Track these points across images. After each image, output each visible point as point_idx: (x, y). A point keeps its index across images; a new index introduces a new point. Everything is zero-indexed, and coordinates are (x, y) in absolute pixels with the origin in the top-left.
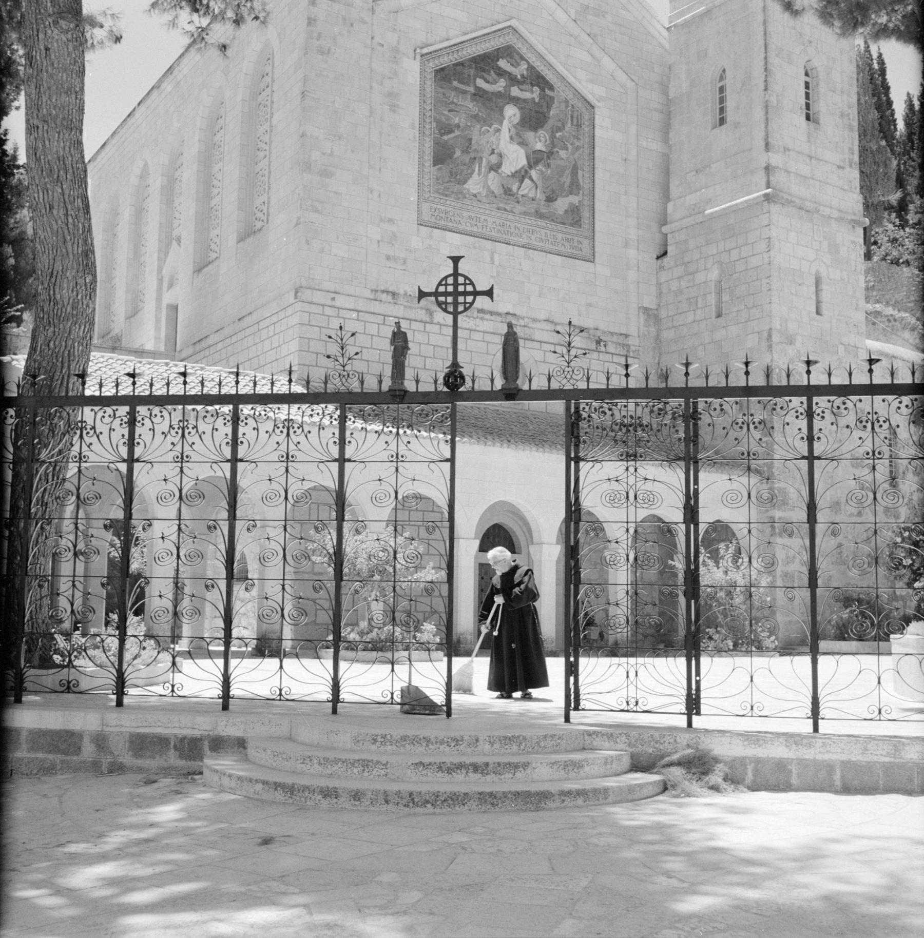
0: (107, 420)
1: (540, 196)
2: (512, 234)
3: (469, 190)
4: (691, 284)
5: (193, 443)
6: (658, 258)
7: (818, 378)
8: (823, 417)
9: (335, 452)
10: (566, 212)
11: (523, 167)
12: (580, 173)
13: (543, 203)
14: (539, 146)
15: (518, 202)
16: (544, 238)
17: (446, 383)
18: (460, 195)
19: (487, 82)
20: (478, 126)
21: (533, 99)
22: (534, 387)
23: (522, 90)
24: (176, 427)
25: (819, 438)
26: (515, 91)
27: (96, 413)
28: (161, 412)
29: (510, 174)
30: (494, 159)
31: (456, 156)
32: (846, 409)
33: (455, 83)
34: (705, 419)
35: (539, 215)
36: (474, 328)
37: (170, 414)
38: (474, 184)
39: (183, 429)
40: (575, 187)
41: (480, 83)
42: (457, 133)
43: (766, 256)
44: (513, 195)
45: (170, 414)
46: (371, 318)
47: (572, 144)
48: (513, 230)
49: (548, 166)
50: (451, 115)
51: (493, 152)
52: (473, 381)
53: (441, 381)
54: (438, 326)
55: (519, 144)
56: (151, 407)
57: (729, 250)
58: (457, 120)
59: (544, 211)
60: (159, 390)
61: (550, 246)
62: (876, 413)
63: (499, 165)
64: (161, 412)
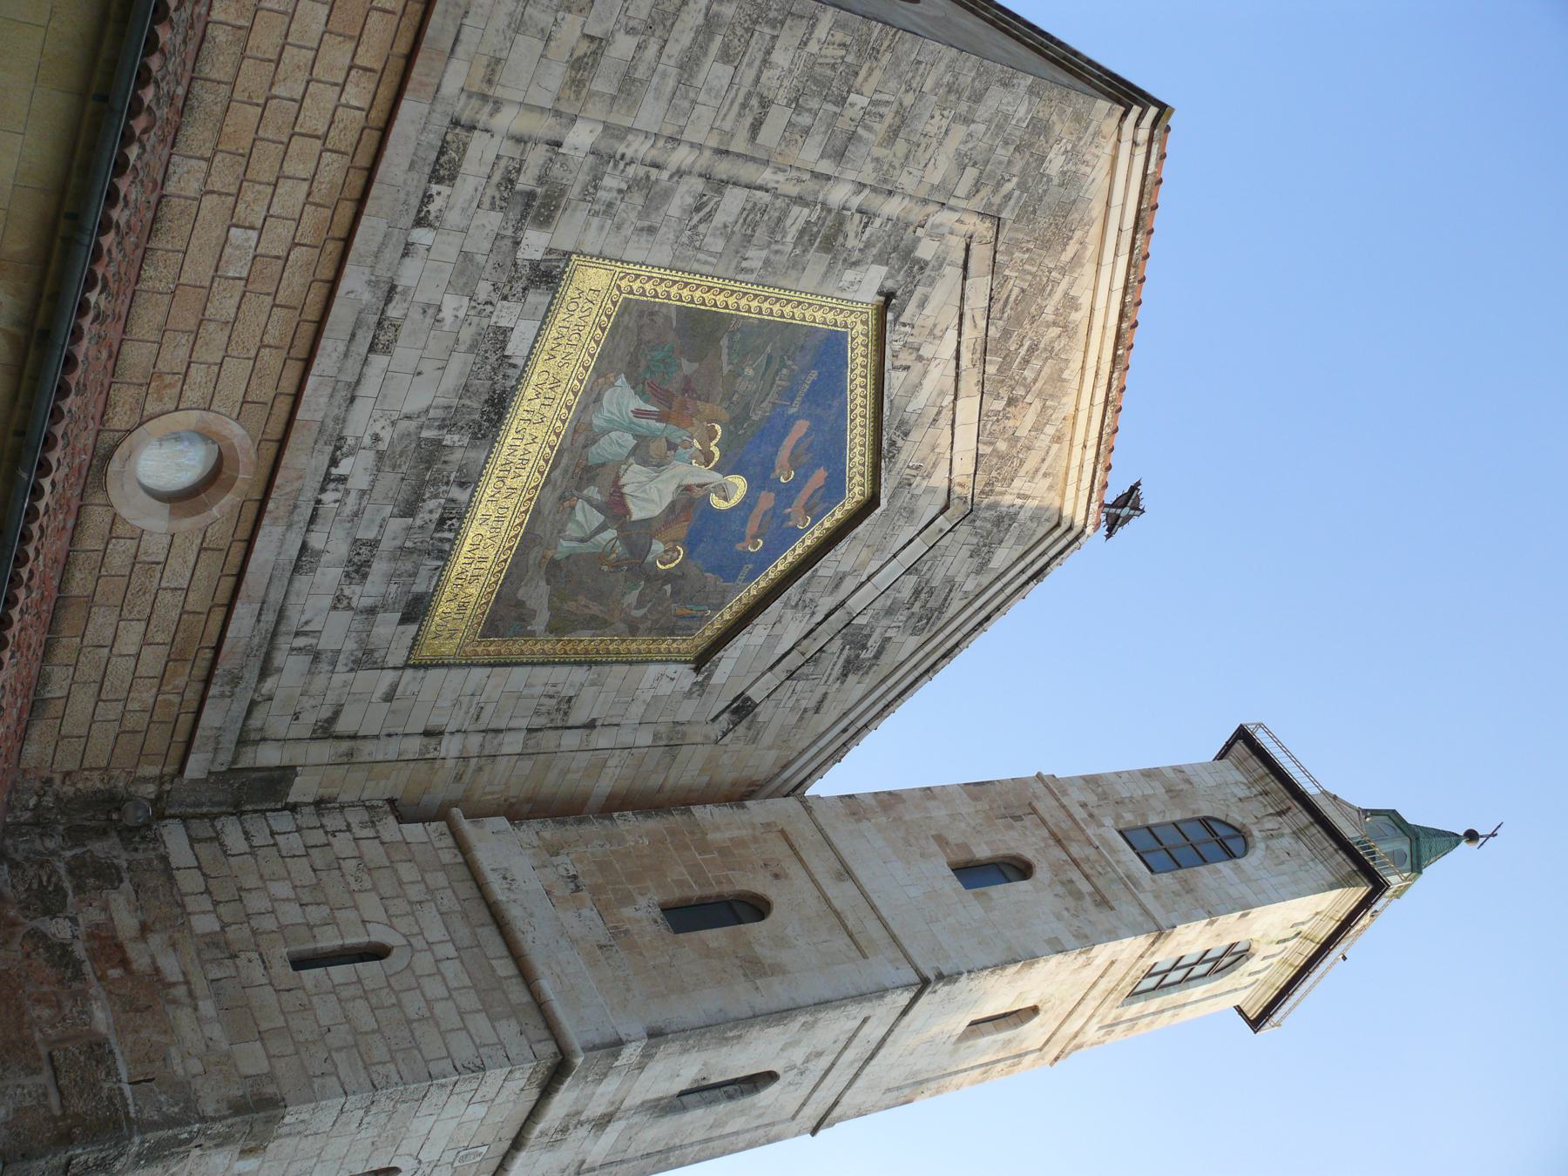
1: (565, 546)
2: (502, 479)
3: (612, 385)
4: (354, 886)
6: (391, 802)
10: (520, 604)
11: (628, 512)
12: (585, 636)
13: (550, 553)
14: (658, 547)
15: (562, 498)
16: (478, 553)
18: (603, 369)
19: (796, 447)
20: (725, 416)
21: (742, 539)
23: (765, 514)
26: (767, 500)
29: (623, 481)
30: (657, 448)
31: (684, 362)
33: (814, 375)
35: (529, 539)
36: (315, 370)
38: (622, 400)
40: (558, 627)
41: (801, 428)
42: (726, 369)
43: (446, 1065)
44: (579, 488)
46: (386, 93)
47: (645, 617)
48: (508, 482)
49: (616, 566)
50: (762, 359)
51: (672, 446)
54: (328, 273)
55: (672, 507)
57: (439, 972)
58: (749, 372)
59: (532, 556)
61: (457, 569)
63: (644, 462)
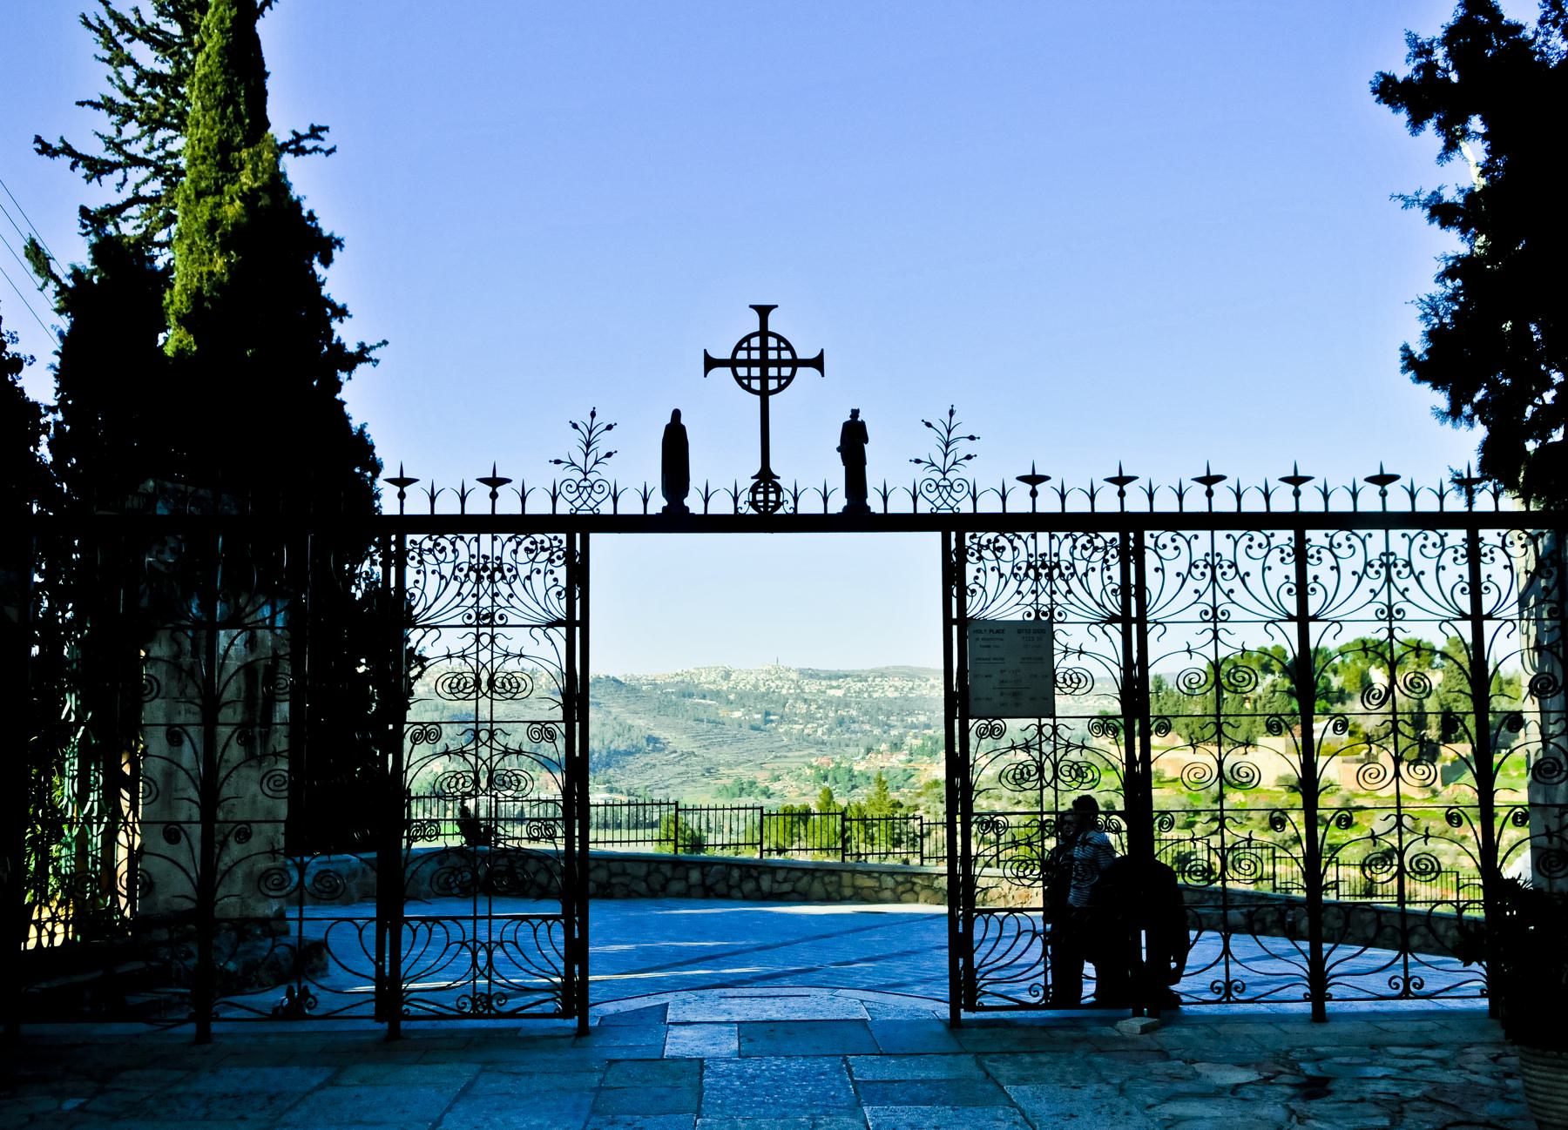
0: (1256, 552)
5: (1231, 591)
7: (1311, 502)
8: (1319, 559)
9: (1291, 605)
17: (754, 504)
22: (893, 509)
24: (1201, 564)
25: (1313, 590)
27: (1236, 543)
28: (1173, 540)
32: (1350, 546)
34: (1151, 560)
37: (1189, 543)
39: (1388, 566)
45: (1189, 543)
52: (796, 499)
53: (745, 497)
56: (1331, 532)
60: (448, 506)
62: (1218, 555)
64: (1173, 540)
